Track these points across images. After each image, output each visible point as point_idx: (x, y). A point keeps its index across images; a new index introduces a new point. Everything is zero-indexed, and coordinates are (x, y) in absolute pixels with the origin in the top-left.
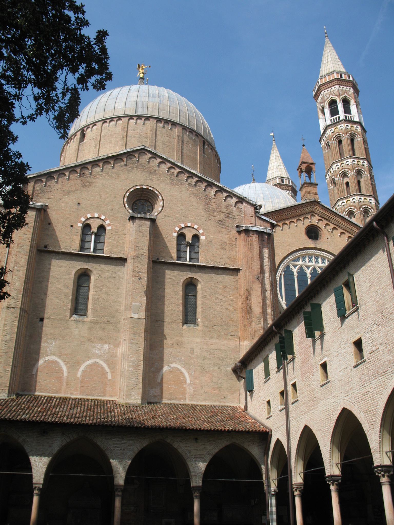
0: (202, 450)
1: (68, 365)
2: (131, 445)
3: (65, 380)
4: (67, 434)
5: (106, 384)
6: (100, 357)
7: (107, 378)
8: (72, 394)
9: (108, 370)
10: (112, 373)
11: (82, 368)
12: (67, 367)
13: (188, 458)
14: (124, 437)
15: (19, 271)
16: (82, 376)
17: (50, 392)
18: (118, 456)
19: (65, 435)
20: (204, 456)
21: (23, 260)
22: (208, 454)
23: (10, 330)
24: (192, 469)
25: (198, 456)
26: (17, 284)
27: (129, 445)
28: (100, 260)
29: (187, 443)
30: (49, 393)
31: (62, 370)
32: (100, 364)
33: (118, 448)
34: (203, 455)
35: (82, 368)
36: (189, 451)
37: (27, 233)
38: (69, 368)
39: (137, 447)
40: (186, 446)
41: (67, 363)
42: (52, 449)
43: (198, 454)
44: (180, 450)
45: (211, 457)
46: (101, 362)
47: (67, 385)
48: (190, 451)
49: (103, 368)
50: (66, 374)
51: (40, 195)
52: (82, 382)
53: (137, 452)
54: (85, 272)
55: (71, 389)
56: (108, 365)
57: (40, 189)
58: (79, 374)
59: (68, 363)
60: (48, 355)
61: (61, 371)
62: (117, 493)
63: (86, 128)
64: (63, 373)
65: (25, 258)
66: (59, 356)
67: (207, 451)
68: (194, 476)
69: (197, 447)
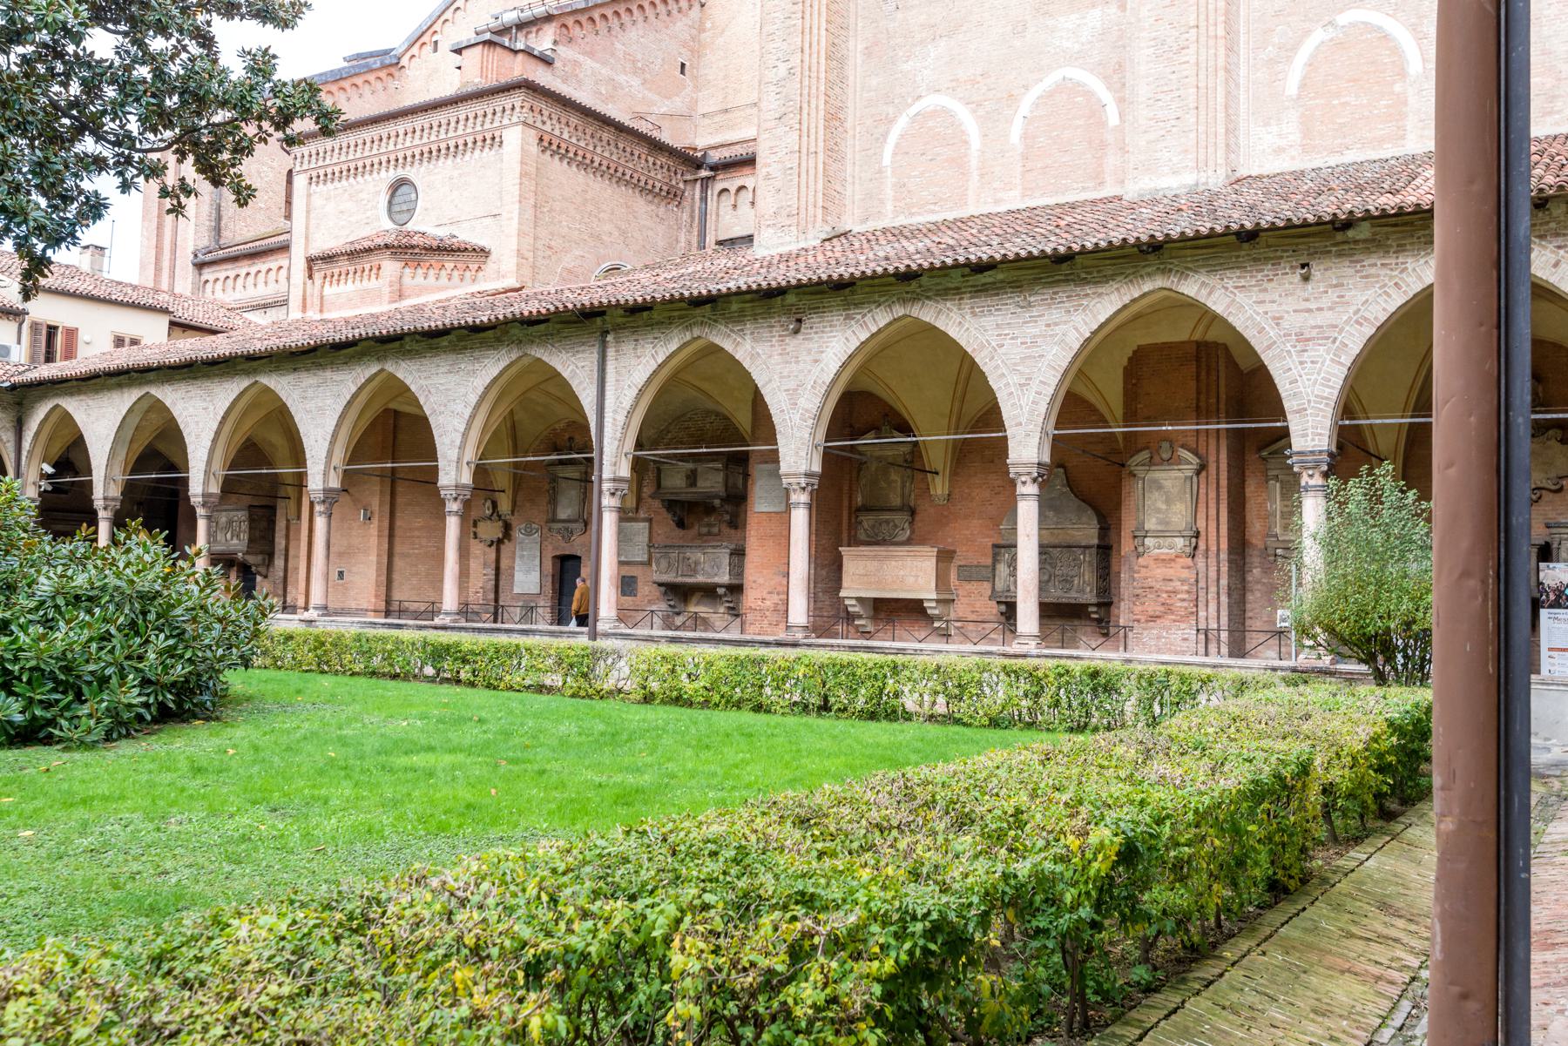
0: (1330, 309)
1: (981, 112)
2: (1056, 324)
3: (974, 163)
4: (859, 317)
5: (1103, 145)
7: (1103, 124)
8: (997, 202)
9: (1106, 96)
10: (1121, 101)
11: (1025, 107)
13: (1269, 347)
14: (1032, 299)
16: (1025, 136)
17: (937, 208)
18: (1015, 364)
19: (853, 322)
20: (1340, 333)
22: (1357, 322)
24: (1287, 386)
25: (1314, 333)
27: (1048, 325)
29: (1266, 290)
30: (933, 212)
33: (1012, 338)
34: (1336, 326)
35: (1025, 107)
36: (1274, 318)
39: (1076, 329)
40: (1262, 302)
42: (822, 370)
43: (1314, 327)
44: (1237, 322)
45: (1369, 331)
47: (982, 176)
48: (1281, 318)
49: (1089, 94)
50: (975, 142)
52: (1025, 157)
53: (1076, 346)
55: (996, 185)
56: (1106, 79)
59: (979, 105)
62: (1021, 489)
67: (1352, 310)
68: (1298, 412)
69: (1307, 300)
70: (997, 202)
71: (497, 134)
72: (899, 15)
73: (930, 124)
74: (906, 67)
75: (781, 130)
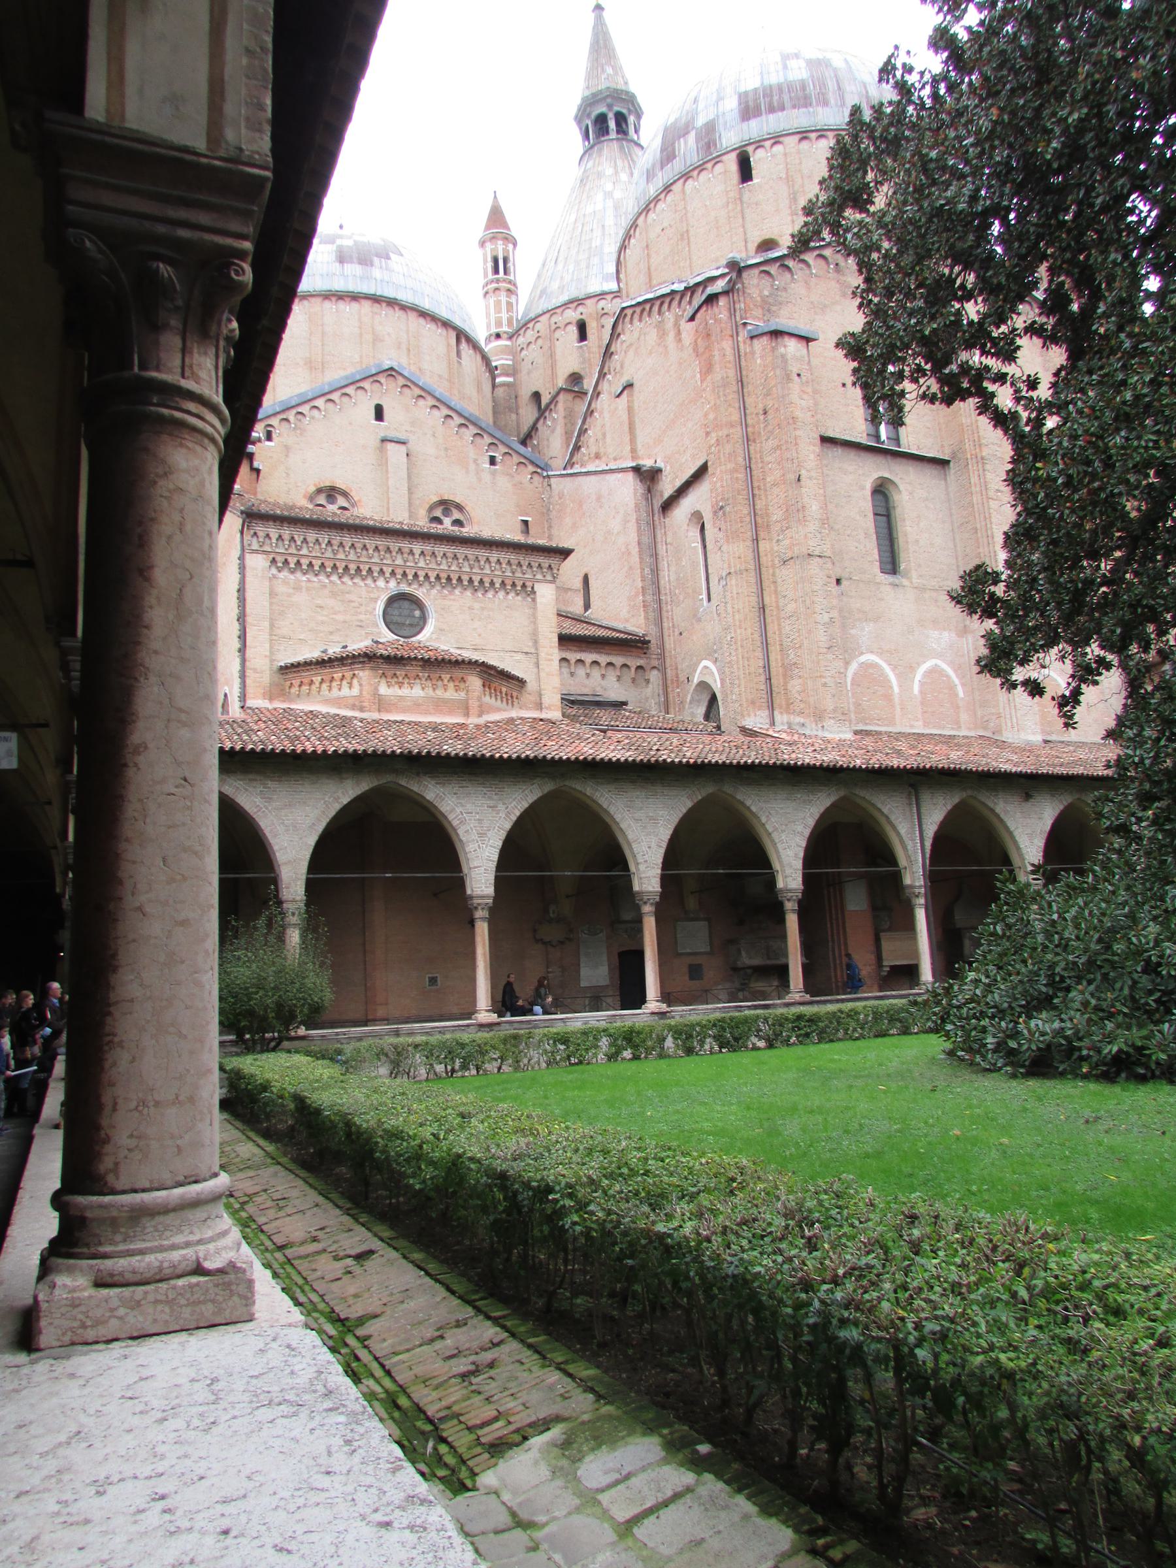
3: (896, 700)
5: (958, 707)
6: (940, 656)
7: (957, 695)
8: (912, 726)
9: (957, 681)
12: (896, 675)
15: (810, 478)
16: (921, 692)
21: (812, 457)
23: (825, 602)
26: (814, 508)
28: (904, 461)
31: (889, 681)
32: (943, 670)
37: (805, 396)
38: (898, 676)
41: (894, 668)
46: (944, 666)
49: (948, 677)
50: (896, 689)
51: (774, 308)
54: (881, 486)
56: (955, 671)
57: (771, 294)
58: (916, 689)
60: (862, 653)
61: (886, 683)
63: (753, 147)
64: (891, 687)
65: (814, 452)
66: (880, 653)
70: (912, 726)
71: (529, 584)
72: (845, 599)
73: (871, 671)
74: (853, 632)
75: (830, 656)
